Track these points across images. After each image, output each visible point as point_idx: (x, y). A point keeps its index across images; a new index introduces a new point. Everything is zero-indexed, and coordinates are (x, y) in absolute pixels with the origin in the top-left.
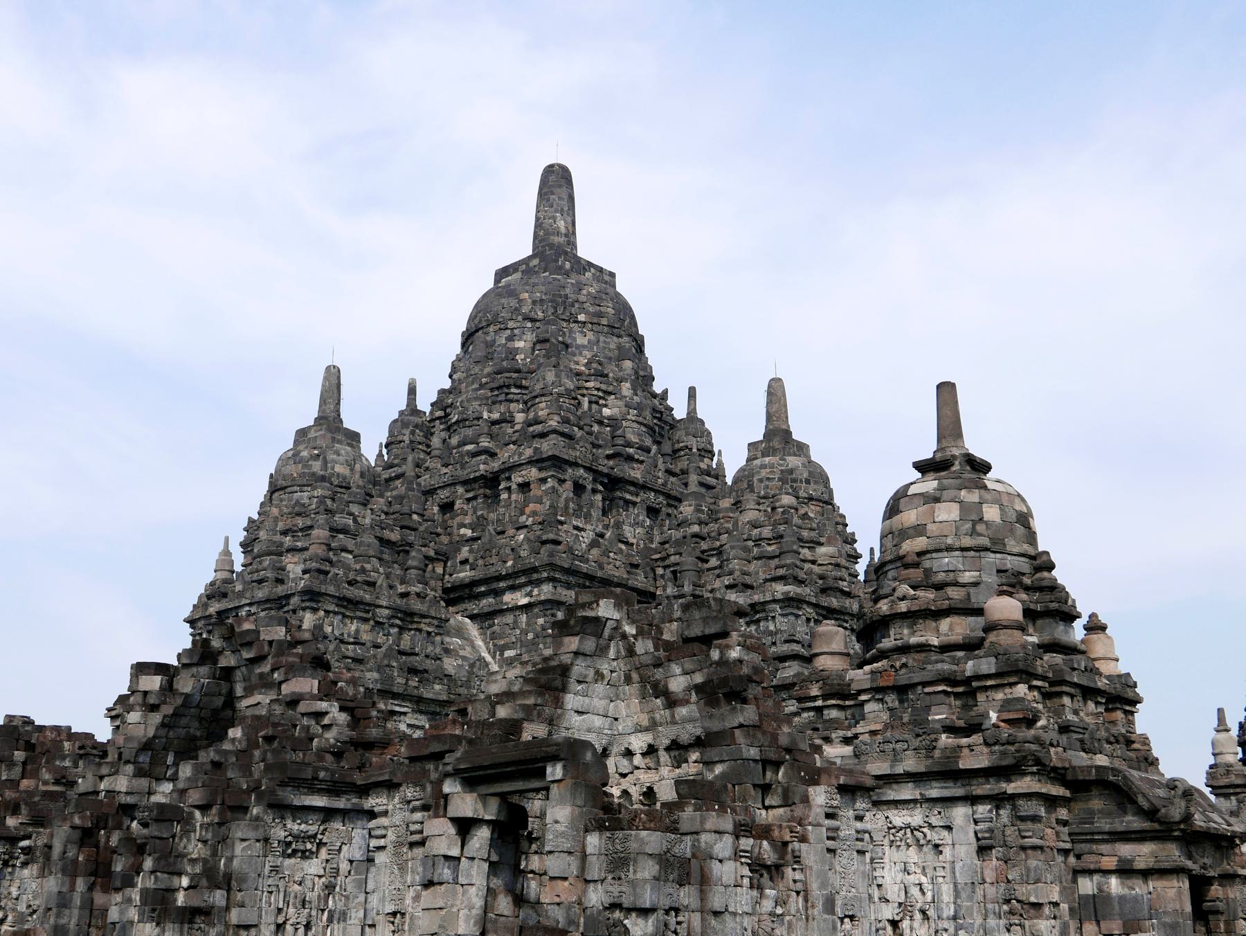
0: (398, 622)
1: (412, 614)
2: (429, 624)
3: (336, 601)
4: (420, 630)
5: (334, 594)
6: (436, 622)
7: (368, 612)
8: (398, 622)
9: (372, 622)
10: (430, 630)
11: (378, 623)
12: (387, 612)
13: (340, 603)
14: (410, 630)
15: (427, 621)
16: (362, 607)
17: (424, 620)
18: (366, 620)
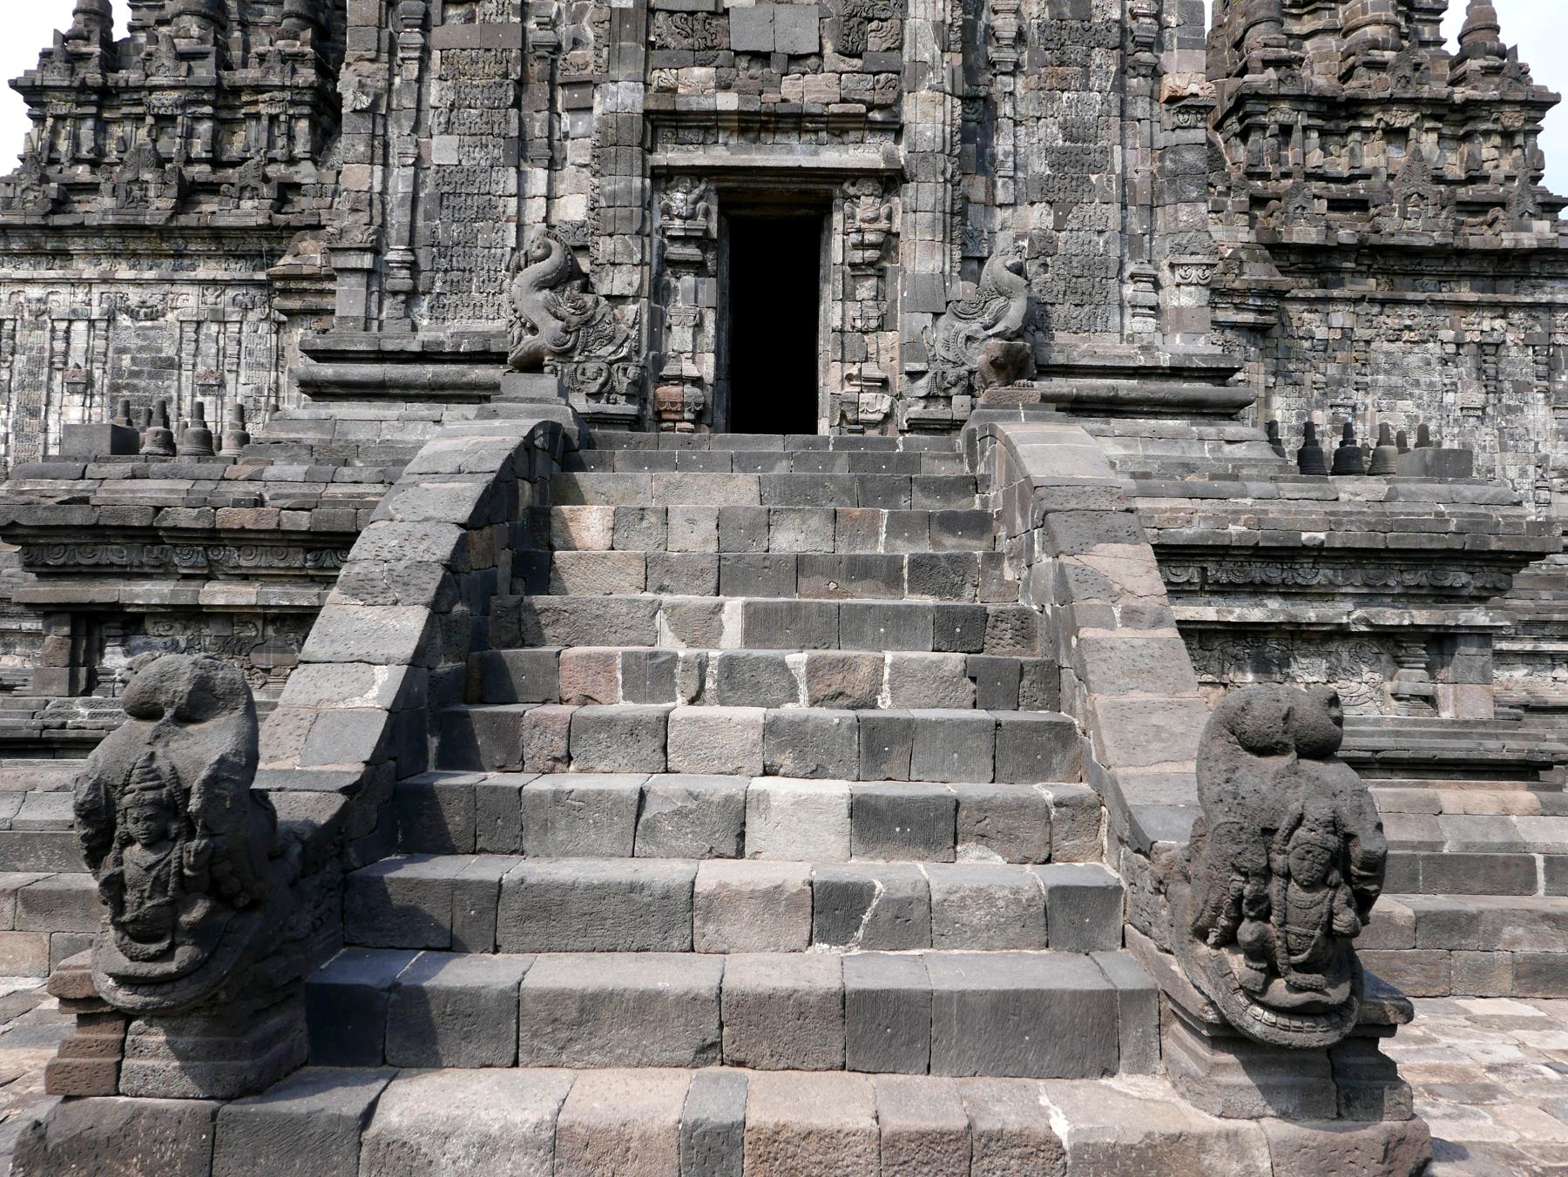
0: (208, 109)
1: (236, 91)
2: (272, 101)
3: (73, 96)
4: (257, 117)
5: (58, 83)
6: (287, 95)
7: (139, 103)
8: (208, 109)
9: (150, 120)
10: (274, 111)
11: (158, 117)
12: (175, 95)
13: (82, 98)
14: (243, 121)
15: (266, 96)
16: (126, 97)
17: (260, 97)
18: (139, 119)
